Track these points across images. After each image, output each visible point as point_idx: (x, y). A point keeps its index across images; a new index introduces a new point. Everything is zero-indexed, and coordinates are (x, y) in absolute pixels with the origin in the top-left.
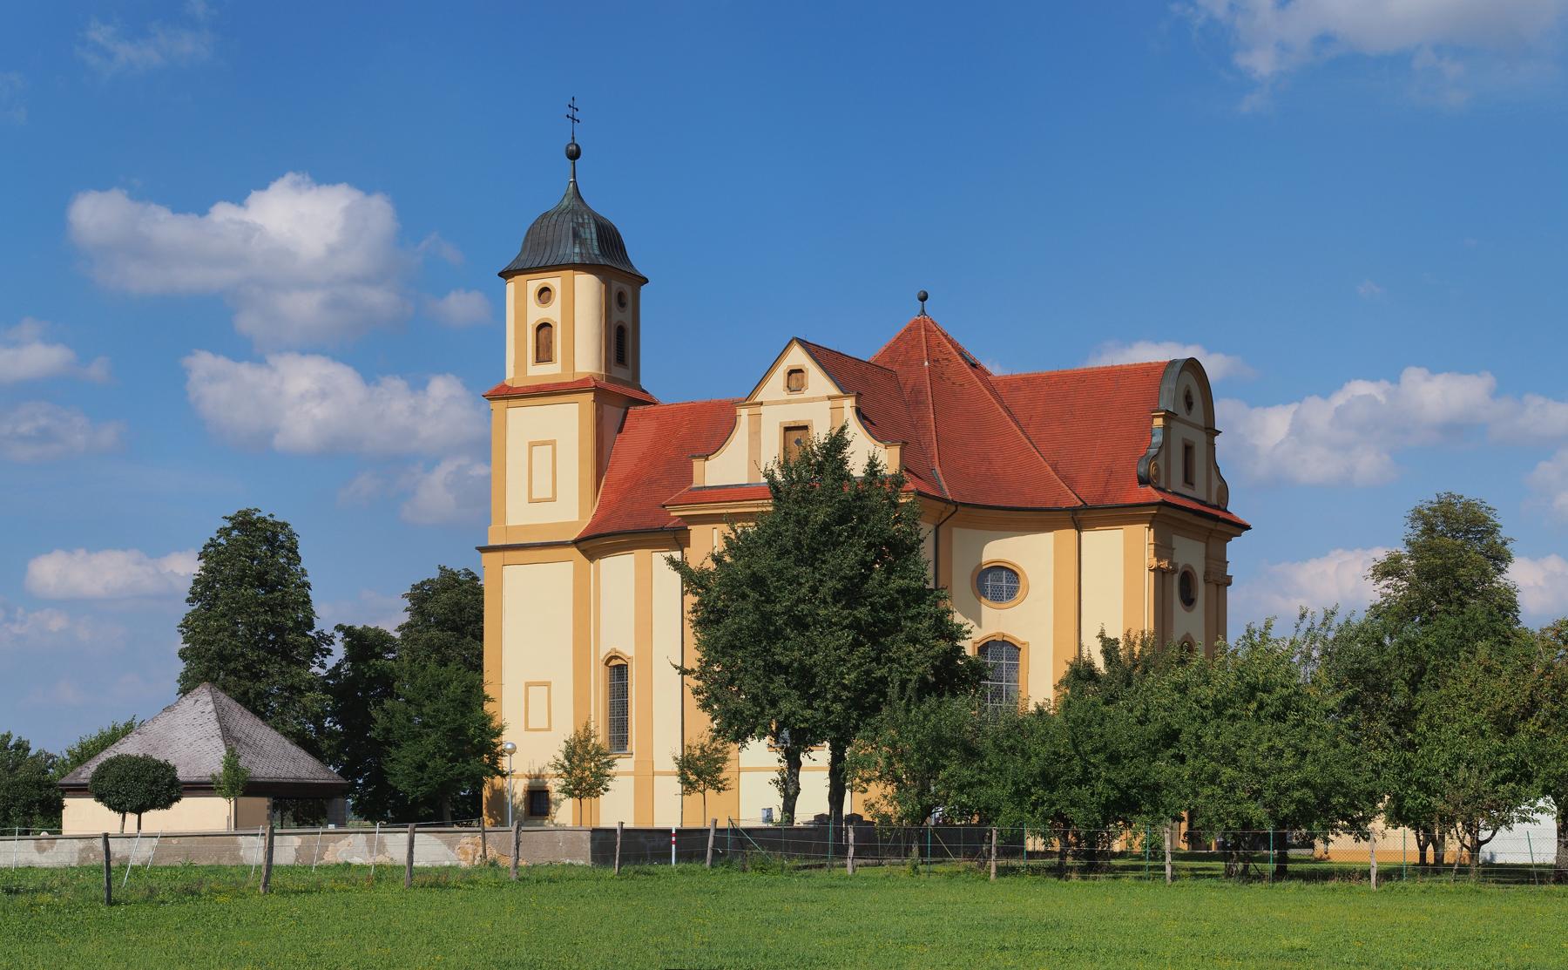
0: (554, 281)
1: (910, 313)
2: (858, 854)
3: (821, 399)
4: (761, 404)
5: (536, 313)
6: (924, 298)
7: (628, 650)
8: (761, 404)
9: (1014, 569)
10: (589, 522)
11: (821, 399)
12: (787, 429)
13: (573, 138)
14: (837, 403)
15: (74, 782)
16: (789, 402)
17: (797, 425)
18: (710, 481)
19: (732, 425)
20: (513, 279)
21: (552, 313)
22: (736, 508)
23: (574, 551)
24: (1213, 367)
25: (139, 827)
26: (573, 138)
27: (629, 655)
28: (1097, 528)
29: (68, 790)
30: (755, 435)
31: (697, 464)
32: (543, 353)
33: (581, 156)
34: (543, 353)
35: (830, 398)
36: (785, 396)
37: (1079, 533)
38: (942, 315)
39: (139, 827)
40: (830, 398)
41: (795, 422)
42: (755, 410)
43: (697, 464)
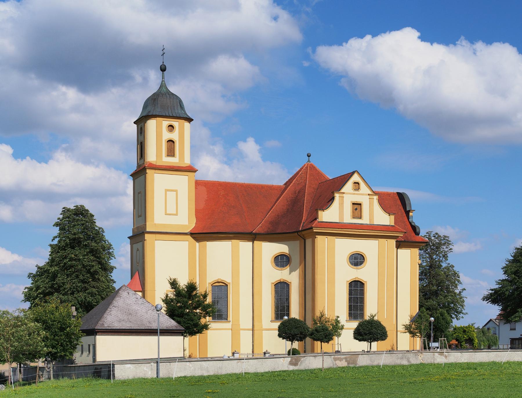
0: (176, 123)
1: (303, 161)
2: (111, 364)
3: (366, 195)
4: (344, 193)
5: (167, 135)
6: (309, 156)
7: (228, 279)
8: (344, 193)
9: (277, 255)
10: (193, 227)
11: (366, 195)
12: (353, 204)
13: (163, 62)
14: (371, 197)
15: (101, 328)
16: (354, 194)
17: (357, 203)
18: (324, 220)
19: (333, 199)
20: (156, 119)
21: (174, 136)
22: (376, 233)
23: (189, 237)
24: (412, 195)
25: (370, 348)
26: (163, 62)
27: (228, 282)
28: (403, 248)
29: (98, 332)
30: (341, 204)
31: (320, 212)
32: (171, 153)
33: (166, 70)
34: (171, 153)
35: (369, 195)
36: (352, 191)
37: (397, 250)
38: (314, 161)
39: (370, 348)
40: (369, 195)
41: (356, 202)
42: (341, 195)
43: (320, 212)
